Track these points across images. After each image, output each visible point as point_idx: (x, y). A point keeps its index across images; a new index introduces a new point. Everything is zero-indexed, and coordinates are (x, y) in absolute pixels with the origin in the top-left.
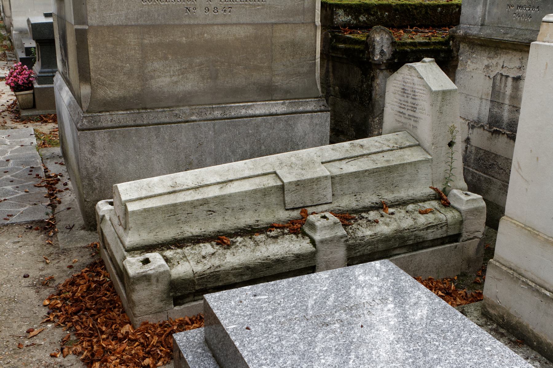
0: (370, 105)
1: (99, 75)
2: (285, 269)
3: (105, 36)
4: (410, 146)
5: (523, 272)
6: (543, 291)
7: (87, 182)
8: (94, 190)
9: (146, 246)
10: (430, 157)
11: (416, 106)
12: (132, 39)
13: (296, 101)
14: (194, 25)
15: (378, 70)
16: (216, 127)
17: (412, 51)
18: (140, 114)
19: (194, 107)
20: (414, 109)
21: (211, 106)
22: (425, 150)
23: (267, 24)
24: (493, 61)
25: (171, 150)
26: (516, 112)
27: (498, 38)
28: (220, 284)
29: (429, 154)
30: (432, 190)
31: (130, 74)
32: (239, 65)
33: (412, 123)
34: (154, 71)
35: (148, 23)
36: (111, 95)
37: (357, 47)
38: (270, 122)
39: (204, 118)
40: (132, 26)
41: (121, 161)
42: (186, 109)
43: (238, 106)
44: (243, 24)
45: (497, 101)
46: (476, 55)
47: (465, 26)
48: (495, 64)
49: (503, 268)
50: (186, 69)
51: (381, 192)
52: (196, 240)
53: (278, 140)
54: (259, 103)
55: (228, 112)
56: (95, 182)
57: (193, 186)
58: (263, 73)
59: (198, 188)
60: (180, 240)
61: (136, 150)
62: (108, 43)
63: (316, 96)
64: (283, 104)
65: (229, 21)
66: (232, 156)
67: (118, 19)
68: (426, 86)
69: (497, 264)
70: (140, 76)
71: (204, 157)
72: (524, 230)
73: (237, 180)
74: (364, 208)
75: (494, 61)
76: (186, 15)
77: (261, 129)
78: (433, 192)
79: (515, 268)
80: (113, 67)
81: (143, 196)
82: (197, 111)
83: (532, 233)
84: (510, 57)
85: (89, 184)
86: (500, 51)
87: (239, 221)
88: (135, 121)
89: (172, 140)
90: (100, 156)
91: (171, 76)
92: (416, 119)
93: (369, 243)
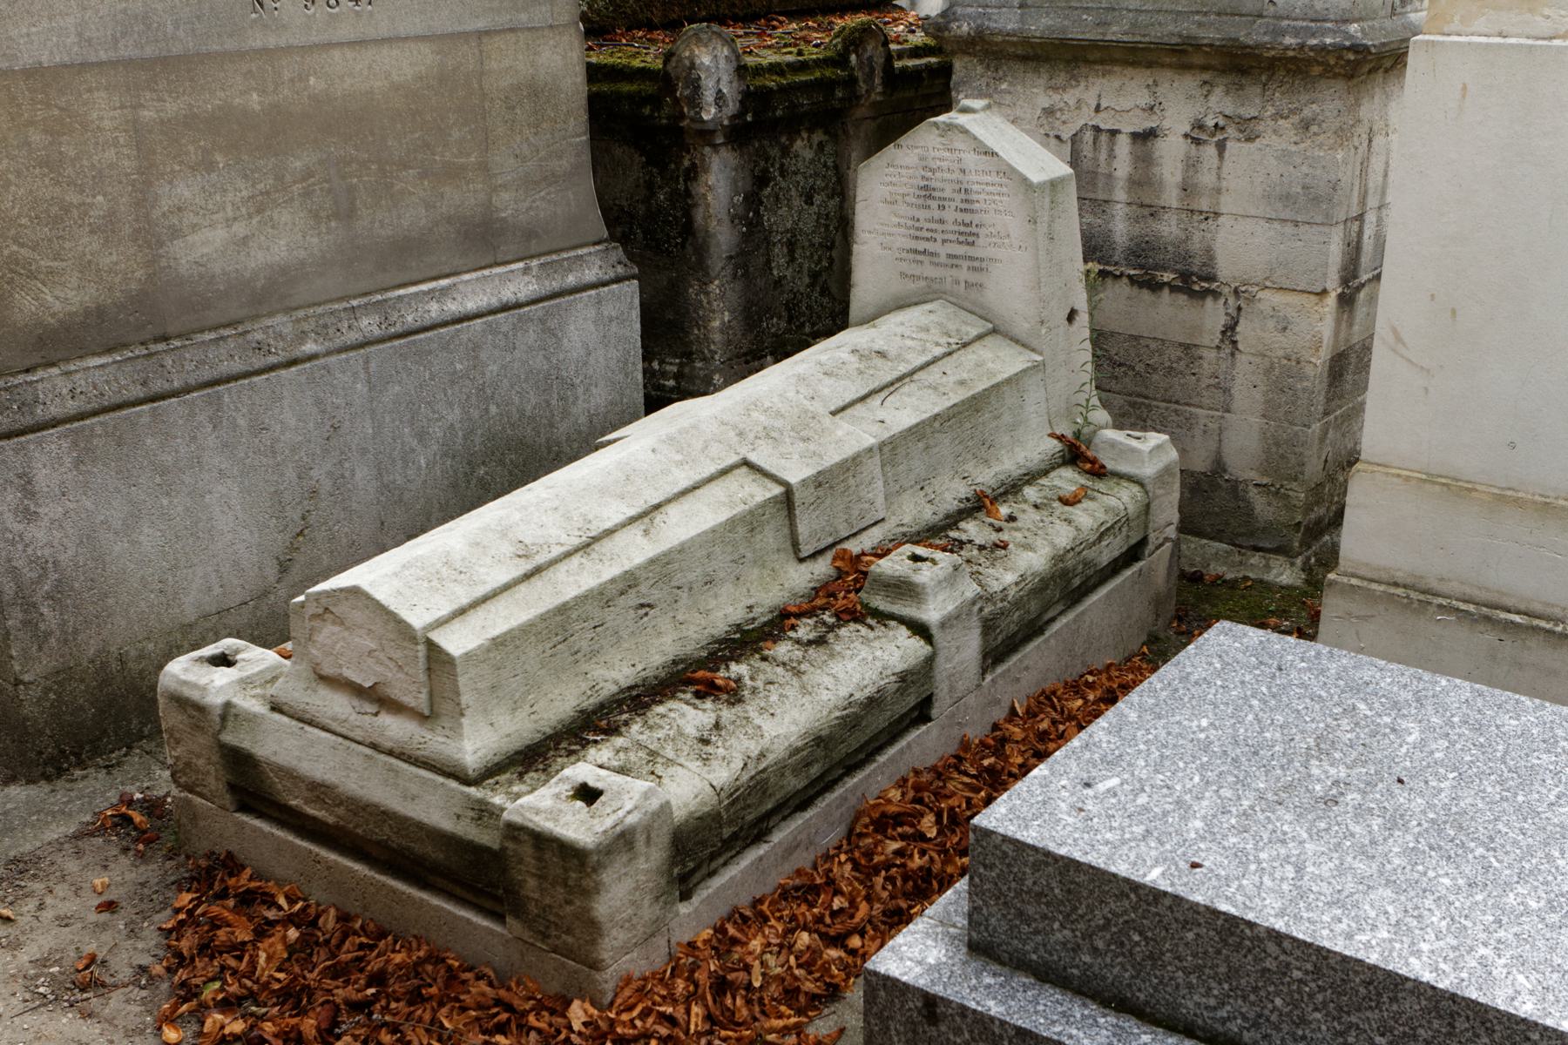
0: (689, 249)
1: (15, 241)
2: (880, 721)
3: (19, 106)
4: (980, 337)
5: (1435, 585)
6: (1503, 615)
7: (20, 616)
8: (42, 639)
9: (517, 753)
10: (1039, 358)
11: (974, 230)
12: (104, 110)
13: (554, 257)
14: (279, 49)
15: (707, 150)
16: (373, 366)
17: (782, 89)
18: (154, 359)
19: (301, 314)
20: (968, 236)
21: (345, 305)
22: (1017, 342)
23: (465, 36)
24: (1066, 97)
25: (256, 463)
26: (1150, 220)
27: (1087, 36)
28: (770, 806)
29: (1033, 350)
30: (1055, 442)
31: (107, 229)
32: (406, 167)
33: (964, 274)
34: (179, 209)
35: (149, 51)
36: (58, 306)
37: (626, 88)
38: (504, 329)
39: (338, 342)
40: (100, 64)
41: (117, 524)
42: (280, 322)
43: (416, 294)
44: (406, 38)
45: (1092, 196)
46: (1011, 84)
47: (969, 10)
48: (1072, 102)
49: (1374, 586)
50: (268, 193)
51: (966, 467)
52: (641, 698)
53: (526, 380)
54: (467, 277)
55: (394, 317)
56: (45, 610)
57: (576, 541)
58: (468, 184)
59: (588, 545)
60: (594, 712)
61: (158, 480)
62: (32, 130)
63: (596, 239)
64: (526, 271)
65: (371, 33)
66: (419, 448)
67: (58, 45)
68: (1009, 172)
69: (1354, 581)
70: (138, 231)
71: (347, 465)
72: (1428, 486)
73: (669, 501)
74: (947, 516)
75: (1070, 97)
76: (255, 21)
77: (483, 356)
78: (1054, 446)
79: (1409, 581)
80: (54, 210)
81: (465, 601)
82: (313, 324)
83: (1452, 488)
84: (1117, 84)
85: (25, 623)
86: (1084, 70)
87: (711, 618)
88: (144, 384)
89: (258, 428)
90: (52, 522)
91: (229, 222)
92: (976, 264)
93: (1018, 604)
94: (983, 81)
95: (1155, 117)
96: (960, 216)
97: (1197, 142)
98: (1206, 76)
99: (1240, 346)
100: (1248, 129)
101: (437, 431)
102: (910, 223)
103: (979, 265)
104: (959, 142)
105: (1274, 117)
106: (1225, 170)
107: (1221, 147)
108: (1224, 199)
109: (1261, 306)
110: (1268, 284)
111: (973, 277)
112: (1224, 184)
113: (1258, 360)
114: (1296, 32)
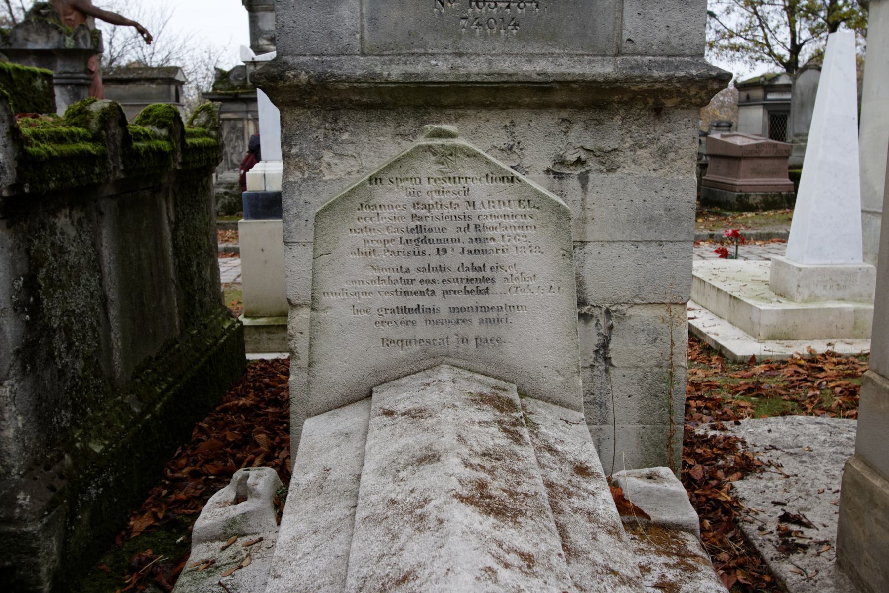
11: (488, 274)
20: (479, 281)
46: (352, 134)
47: (302, 59)
92: (492, 315)
94: (321, 133)
95: (515, 157)
96: (467, 260)
97: (559, 176)
98: (565, 114)
99: (614, 362)
100: (608, 160)
102: (395, 276)
103: (495, 317)
104: (466, 168)
105: (632, 149)
107: (584, 179)
108: (589, 228)
109: (631, 322)
110: (637, 301)
111: (486, 332)
112: (589, 214)
113: (632, 372)
114: (661, 66)
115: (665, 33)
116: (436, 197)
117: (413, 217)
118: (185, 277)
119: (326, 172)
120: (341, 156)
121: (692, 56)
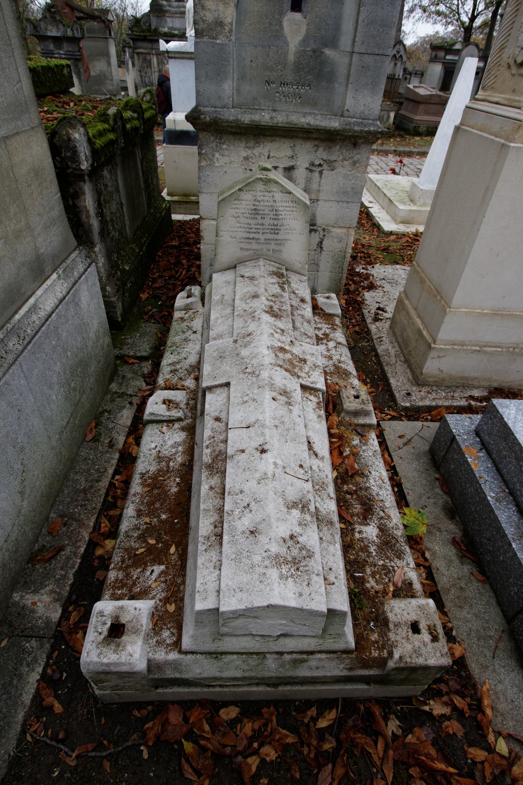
11: (279, 227)
15: (82, 183)
20: (275, 230)
24: (254, 151)
46: (228, 145)
71: (30, 424)
75: (256, 151)
92: (279, 242)
94: (214, 144)
96: (272, 222)
97: (311, 171)
98: (316, 143)
100: (331, 164)
101: (55, 379)
102: (246, 226)
103: (280, 243)
105: (342, 161)
106: (322, 182)
107: (321, 173)
108: (321, 194)
109: (332, 234)
111: (276, 248)
112: (321, 188)
114: (359, 124)
115: (363, 108)
116: (262, 198)
117: (254, 205)
118: (147, 185)
119: (216, 162)
120: (223, 155)
121: (373, 120)
